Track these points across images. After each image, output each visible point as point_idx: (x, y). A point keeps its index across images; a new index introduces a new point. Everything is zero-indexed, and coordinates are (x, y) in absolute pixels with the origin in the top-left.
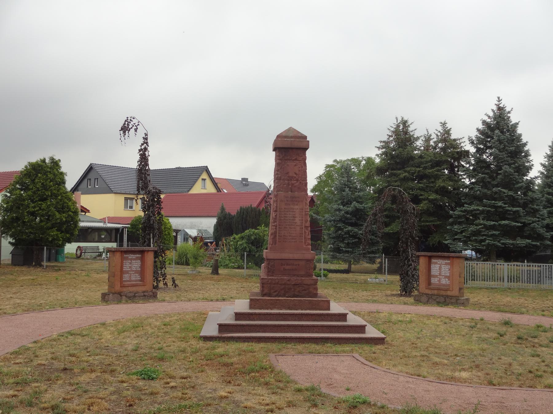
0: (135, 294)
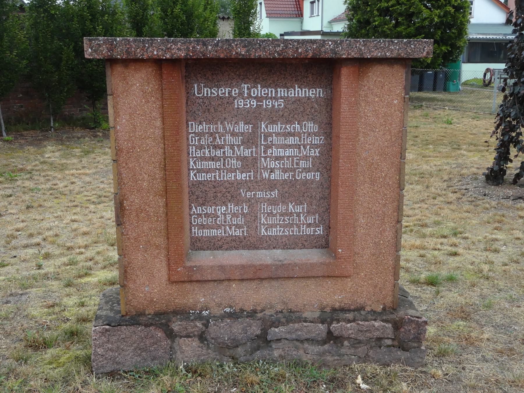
0: (269, 324)
